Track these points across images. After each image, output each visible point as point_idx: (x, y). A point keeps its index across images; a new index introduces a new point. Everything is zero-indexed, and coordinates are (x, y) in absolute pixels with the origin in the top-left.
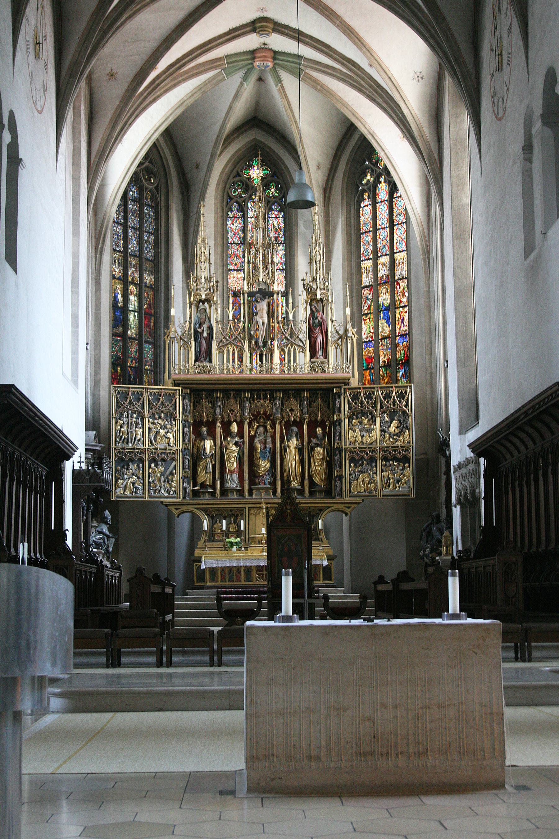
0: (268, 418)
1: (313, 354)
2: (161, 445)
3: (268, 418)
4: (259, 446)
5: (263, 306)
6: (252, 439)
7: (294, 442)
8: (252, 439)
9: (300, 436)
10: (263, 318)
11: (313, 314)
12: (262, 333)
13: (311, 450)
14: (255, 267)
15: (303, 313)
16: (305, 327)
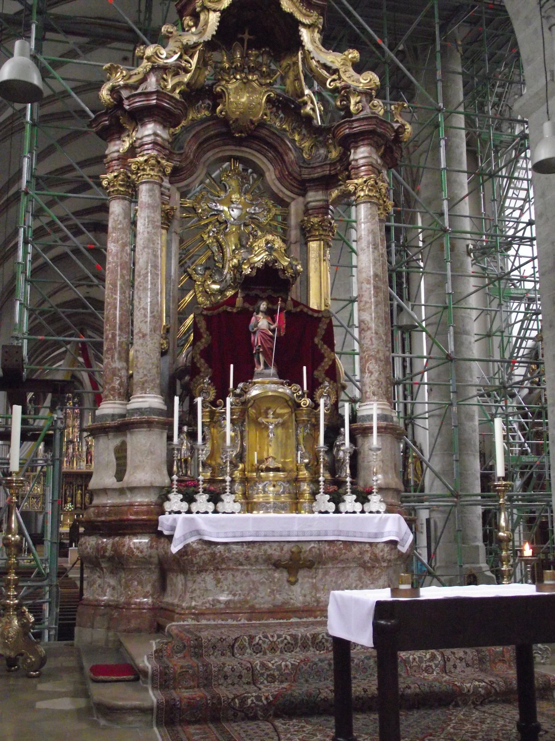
0: (71, 483)
1: (87, 462)
2: (36, 492)
3: (71, 483)
4: (68, 493)
5: (71, 446)
6: (66, 490)
7: (80, 491)
8: (66, 490)
9: (82, 490)
10: (71, 450)
11: (88, 449)
12: (70, 455)
13: (85, 495)
14: (69, 433)
15: (85, 449)
16: (85, 454)
